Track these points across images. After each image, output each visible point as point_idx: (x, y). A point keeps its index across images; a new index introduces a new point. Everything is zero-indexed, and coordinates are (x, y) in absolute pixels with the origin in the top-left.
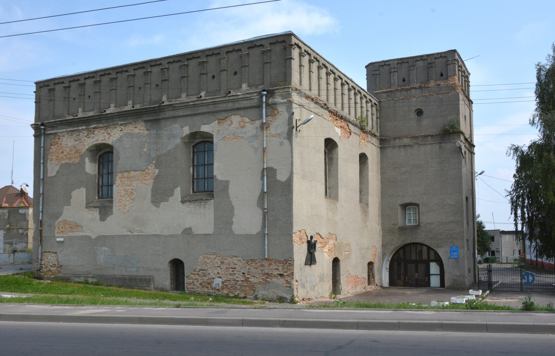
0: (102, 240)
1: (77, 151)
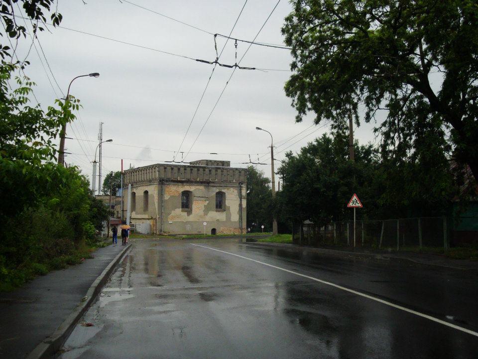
0: (187, 223)
1: (178, 192)
